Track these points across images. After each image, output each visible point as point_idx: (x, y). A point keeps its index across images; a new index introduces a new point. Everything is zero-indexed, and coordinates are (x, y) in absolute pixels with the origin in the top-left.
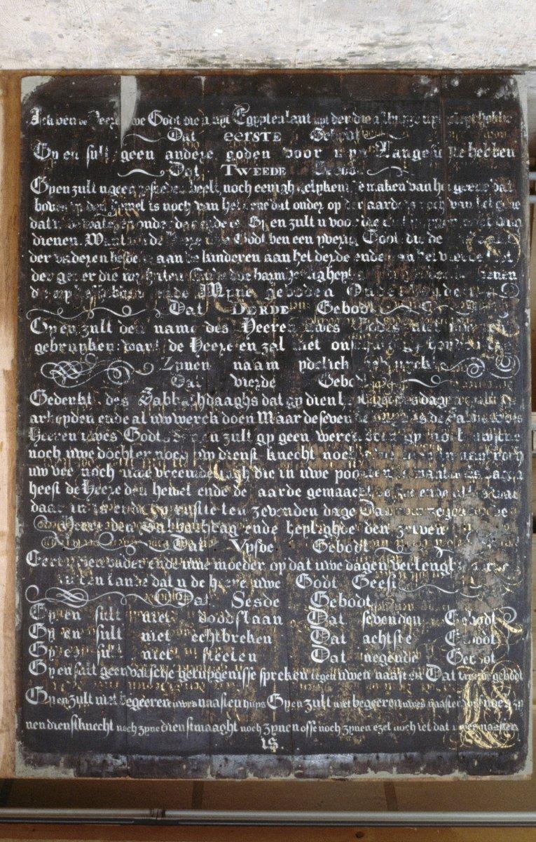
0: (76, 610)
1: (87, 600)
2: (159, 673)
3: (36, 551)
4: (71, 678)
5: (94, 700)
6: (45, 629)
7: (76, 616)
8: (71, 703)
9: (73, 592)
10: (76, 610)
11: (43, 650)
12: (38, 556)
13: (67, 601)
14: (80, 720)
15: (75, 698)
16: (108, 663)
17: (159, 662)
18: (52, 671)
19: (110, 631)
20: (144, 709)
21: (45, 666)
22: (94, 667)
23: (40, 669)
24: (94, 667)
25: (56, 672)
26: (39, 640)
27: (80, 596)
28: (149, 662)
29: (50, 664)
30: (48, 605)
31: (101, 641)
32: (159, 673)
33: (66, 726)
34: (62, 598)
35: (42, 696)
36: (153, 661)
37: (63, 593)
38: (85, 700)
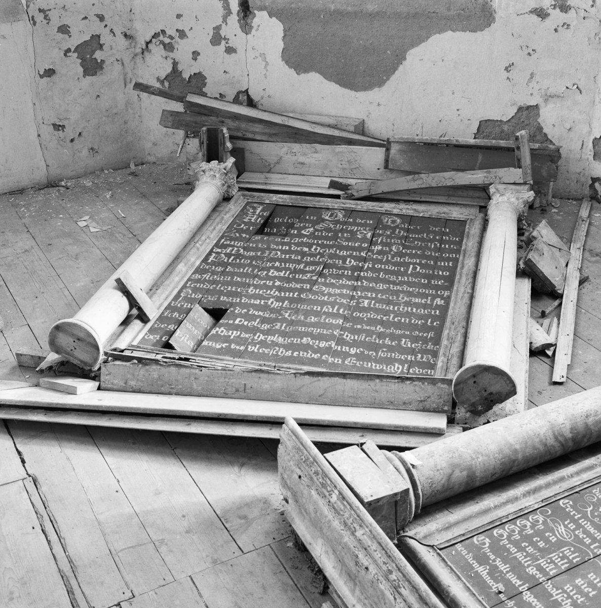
0: (556, 536)
1: (569, 540)
2: (563, 600)
3: (571, 503)
4: (511, 553)
5: (507, 572)
6: (528, 527)
7: (553, 539)
8: (494, 561)
9: (565, 530)
10: (556, 536)
11: (515, 532)
12: (570, 505)
13: (558, 531)
14: (487, 571)
15: (499, 561)
16: (540, 569)
17: (571, 597)
18: (506, 542)
19: (562, 560)
20: (530, 604)
21: (505, 537)
22: (529, 563)
23: (502, 536)
24: (529, 563)
25: (507, 544)
26: (518, 527)
27: (567, 535)
28: (565, 592)
29: (509, 538)
30: (545, 523)
31: (550, 558)
32: (563, 600)
33: (476, 565)
34: (558, 528)
35: (485, 544)
36: (568, 594)
37: (560, 526)
38: (503, 568)
